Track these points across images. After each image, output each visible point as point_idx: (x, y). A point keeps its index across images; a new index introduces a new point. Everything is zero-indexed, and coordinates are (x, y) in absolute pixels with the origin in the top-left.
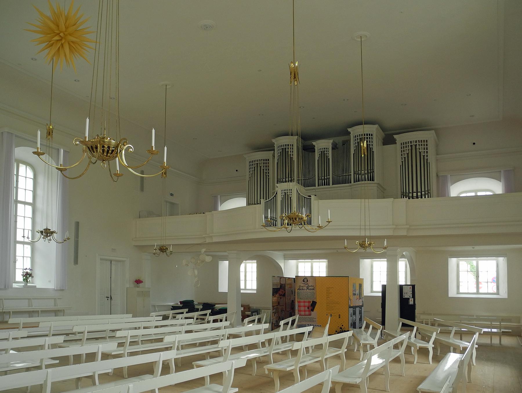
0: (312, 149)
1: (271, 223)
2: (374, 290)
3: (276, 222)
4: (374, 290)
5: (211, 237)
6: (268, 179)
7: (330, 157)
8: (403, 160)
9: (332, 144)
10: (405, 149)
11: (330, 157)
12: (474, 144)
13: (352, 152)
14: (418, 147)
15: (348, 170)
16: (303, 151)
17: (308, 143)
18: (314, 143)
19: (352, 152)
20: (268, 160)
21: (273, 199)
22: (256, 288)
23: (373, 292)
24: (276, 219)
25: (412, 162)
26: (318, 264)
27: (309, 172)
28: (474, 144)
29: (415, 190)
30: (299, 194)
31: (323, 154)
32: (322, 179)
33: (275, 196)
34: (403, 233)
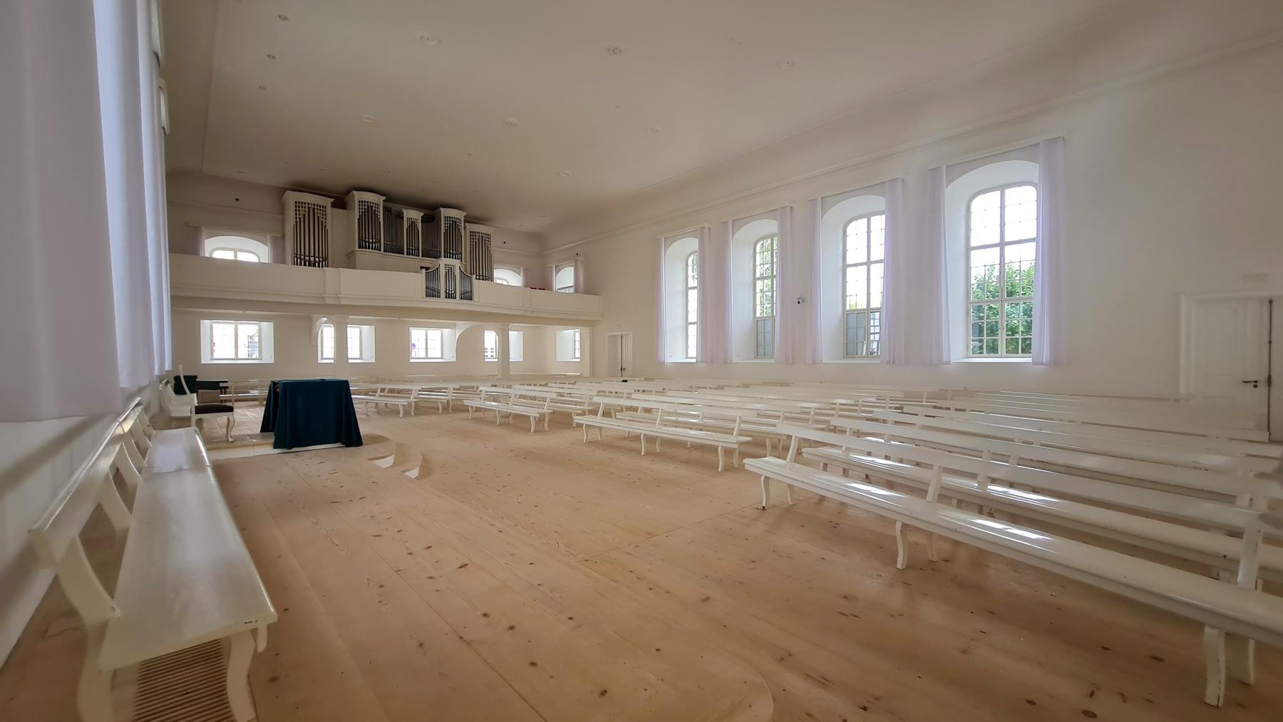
0: (400, 216)
1: (432, 293)
2: (690, 355)
4: (690, 355)
5: (339, 298)
7: (420, 229)
11: (420, 229)
14: (484, 239)
15: (438, 246)
17: (395, 207)
18: (404, 211)
22: (695, 356)
26: (416, 331)
29: (481, 274)
32: (412, 249)
34: (528, 314)
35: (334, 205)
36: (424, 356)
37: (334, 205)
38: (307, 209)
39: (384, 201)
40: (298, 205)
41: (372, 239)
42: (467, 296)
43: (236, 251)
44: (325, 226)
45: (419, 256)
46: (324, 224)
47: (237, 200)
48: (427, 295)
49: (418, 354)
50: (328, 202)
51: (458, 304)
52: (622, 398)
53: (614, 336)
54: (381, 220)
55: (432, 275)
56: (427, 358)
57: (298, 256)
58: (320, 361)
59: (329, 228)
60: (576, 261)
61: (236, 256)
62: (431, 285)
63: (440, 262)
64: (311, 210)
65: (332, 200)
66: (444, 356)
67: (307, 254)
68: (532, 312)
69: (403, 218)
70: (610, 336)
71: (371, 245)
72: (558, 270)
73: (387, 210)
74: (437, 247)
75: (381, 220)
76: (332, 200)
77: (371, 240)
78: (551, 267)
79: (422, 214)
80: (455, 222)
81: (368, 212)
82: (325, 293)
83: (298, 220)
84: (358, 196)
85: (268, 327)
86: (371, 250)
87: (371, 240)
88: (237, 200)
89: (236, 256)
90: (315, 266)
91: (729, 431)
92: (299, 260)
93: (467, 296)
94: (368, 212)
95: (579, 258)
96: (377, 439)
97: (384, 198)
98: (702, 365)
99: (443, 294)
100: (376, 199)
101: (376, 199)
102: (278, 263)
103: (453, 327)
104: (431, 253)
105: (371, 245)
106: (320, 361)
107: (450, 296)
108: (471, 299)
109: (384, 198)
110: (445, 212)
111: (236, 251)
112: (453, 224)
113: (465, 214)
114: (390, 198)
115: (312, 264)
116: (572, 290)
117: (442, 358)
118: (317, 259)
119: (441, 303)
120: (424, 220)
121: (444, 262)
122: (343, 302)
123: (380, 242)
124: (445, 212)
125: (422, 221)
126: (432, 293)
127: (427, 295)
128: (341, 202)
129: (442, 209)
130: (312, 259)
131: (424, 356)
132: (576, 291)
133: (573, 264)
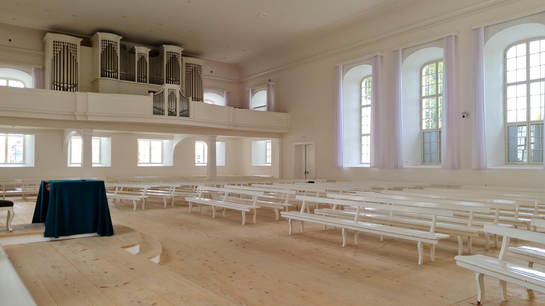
0: (133, 51)
1: (158, 111)
3: (163, 112)
6: (76, 62)
7: (148, 62)
8: (187, 75)
9: (149, 52)
10: (189, 68)
11: (148, 62)
12: (212, 72)
13: (165, 63)
15: (161, 74)
16: (124, 49)
17: (129, 45)
18: (136, 47)
19: (165, 63)
20: (76, 45)
21: (160, 94)
23: (362, 164)
24: (163, 110)
25: (197, 77)
27: (130, 69)
28: (212, 72)
30: (181, 94)
31: (142, 58)
32: (142, 77)
33: (162, 92)
34: (231, 128)
35: (83, 44)
36: (148, 162)
37: (83, 44)
38: (62, 47)
39: (121, 40)
40: (56, 44)
41: (112, 69)
42: (185, 114)
43: (8, 79)
44: (76, 60)
45: (146, 83)
46: (75, 58)
47: (10, 40)
48: (154, 114)
49: (143, 160)
50: (78, 41)
51: (177, 120)
52: (315, 196)
53: (299, 146)
54: (119, 55)
55: (158, 98)
56: (150, 163)
57: (55, 83)
58: (69, 165)
59: (78, 61)
60: (269, 85)
61: (8, 83)
62: (157, 105)
63: (164, 87)
64: (66, 47)
65: (81, 40)
66: (165, 161)
67: (62, 82)
68: (234, 126)
69: (135, 53)
70: (296, 146)
71: (110, 74)
72: (254, 92)
73: (123, 47)
74: (160, 76)
75: (119, 55)
76: (81, 40)
77: (110, 71)
78: (248, 91)
79: (150, 50)
80: (175, 56)
81: (109, 48)
82: (76, 112)
83: (55, 55)
84: (101, 36)
85: (30, 138)
86: (110, 78)
87: (110, 71)
88: (10, 40)
89: (8, 83)
90: (67, 90)
91: (426, 228)
92: (55, 86)
93: (185, 114)
94: (109, 48)
95: (271, 83)
96: (126, 230)
97: (121, 38)
98: (376, 169)
99: (166, 112)
100: (115, 38)
101: (115, 38)
102: (40, 88)
103: (172, 138)
104: (156, 80)
105: (110, 74)
106: (69, 165)
107: (171, 114)
108: (187, 116)
109: (121, 38)
110: (167, 48)
111: (8, 79)
112: (173, 58)
113: (182, 49)
114: (125, 38)
115: (65, 89)
116: (264, 109)
117: (162, 163)
118: (69, 86)
119: (165, 119)
120: (151, 54)
121: (167, 87)
122: (90, 119)
123: (117, 72)
124: (167, 48)
125: (150, 56)
126: (158, 111)
127: (154, 114)
128: (88, 42)
129: (164, 46)
130: (66, 85)
131: (148, 162)
132: (269, 109)
133: (266, 88)
